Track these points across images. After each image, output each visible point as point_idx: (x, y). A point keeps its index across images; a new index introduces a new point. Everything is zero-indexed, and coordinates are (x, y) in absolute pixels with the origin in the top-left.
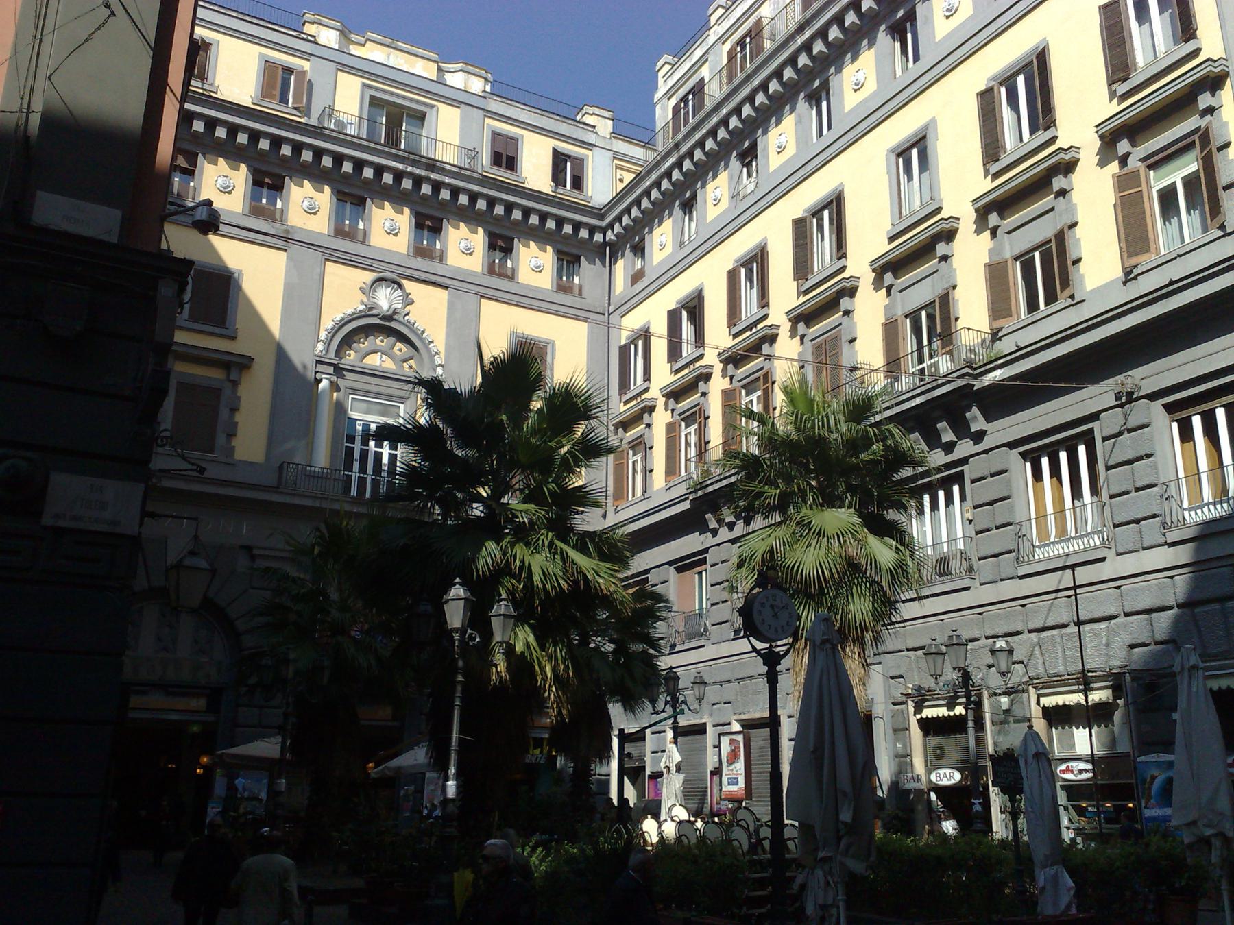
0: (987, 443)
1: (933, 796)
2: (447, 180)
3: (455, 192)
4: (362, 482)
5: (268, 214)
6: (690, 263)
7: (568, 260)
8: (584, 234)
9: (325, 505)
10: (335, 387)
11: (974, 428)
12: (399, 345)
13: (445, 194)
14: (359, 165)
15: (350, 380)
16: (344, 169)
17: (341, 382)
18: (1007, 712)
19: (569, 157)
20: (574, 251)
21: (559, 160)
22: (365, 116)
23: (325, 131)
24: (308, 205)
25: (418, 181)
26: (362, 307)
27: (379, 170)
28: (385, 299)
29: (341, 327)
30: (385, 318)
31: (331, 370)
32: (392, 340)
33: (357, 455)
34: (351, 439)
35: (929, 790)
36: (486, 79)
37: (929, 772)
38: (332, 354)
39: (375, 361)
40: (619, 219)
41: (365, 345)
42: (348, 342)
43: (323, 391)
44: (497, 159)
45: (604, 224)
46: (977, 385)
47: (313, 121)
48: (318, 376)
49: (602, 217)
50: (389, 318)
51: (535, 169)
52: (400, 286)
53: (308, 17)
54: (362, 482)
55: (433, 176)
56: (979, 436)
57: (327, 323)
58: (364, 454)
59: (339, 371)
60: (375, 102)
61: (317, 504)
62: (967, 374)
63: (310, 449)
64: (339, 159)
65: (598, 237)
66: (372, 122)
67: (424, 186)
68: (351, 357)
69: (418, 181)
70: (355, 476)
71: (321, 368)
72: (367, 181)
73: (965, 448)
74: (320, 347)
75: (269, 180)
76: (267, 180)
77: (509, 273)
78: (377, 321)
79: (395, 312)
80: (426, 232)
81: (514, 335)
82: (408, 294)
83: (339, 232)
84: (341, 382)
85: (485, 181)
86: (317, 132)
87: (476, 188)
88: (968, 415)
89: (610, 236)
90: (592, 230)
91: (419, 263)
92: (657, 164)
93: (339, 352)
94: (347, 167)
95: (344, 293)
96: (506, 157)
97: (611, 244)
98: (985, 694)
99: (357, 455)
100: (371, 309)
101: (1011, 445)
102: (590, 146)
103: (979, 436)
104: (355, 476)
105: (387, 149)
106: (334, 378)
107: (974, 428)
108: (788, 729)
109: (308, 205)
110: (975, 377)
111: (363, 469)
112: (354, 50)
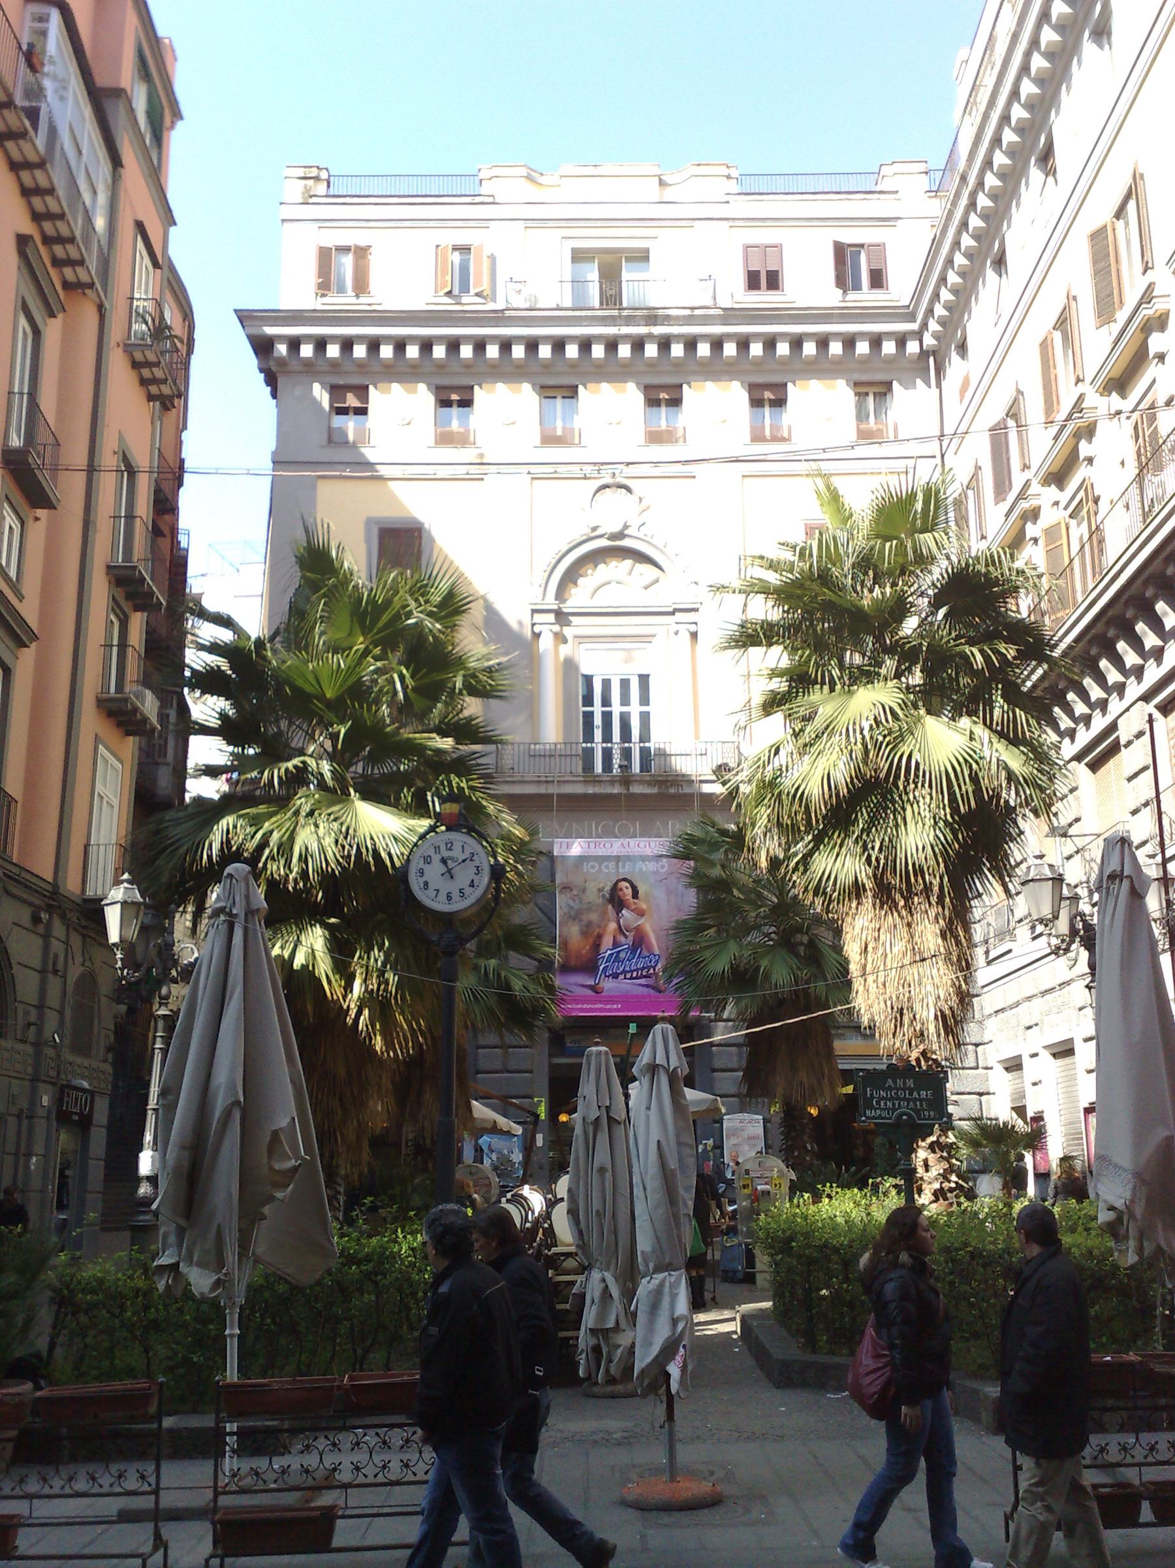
3: (691, 344)
4: (607, 755)
6: (1009, 347)
7: (874, 389)
8: (889, 347)
9: (553, 790)
10: (560, 638)
13: (677, 350)
14: (559, 345)
17: (568, 632)
19: (862, 246)
21: (844, 255)
23: (508, 313)
25: (638, 345)
27: (585, 345)
28: (612, 513)
31: (551, 618)
32: (628, 563)
33: (598, 720)
34: (588, 700)
39: (608, 599)
40: (930, 311)
42: (571, 577)
44: (753, 281)
45: (914, 326)
47: (500, 305)
48: (537, 629)
49: (911, 317)
50: (620, 535)
51: (810, 283)
52: (629, 490)
54: (607, 755)
58: (607, 717)
60: (578, 256)
61: (542, 790)
64: (532, 345)
65: (913, 347)
66: (578, 283)
68: (578, 598)
69: (638, 345)
70: (598, 746)
71: (538, 618)
75: (454, 396)
76: (663, 396)
77: (785, 435)
78: (604, 543)
79: (626, 527)
80: (767, 410)
81: (369, 522)
84: (568, 632)
85: (730, 315)
86: (498, 317)
87: (717, 330)
89: (929, 340)
90: (901, 341)
92: (950, 214)
93: (560, 594)
94: (863, 348)
96: (764, 278)
99: (598, 720)
100: (594, 529)
104: (598, 746)
106: (557, 628)
108: (68, 1013)
111: (607, 738)
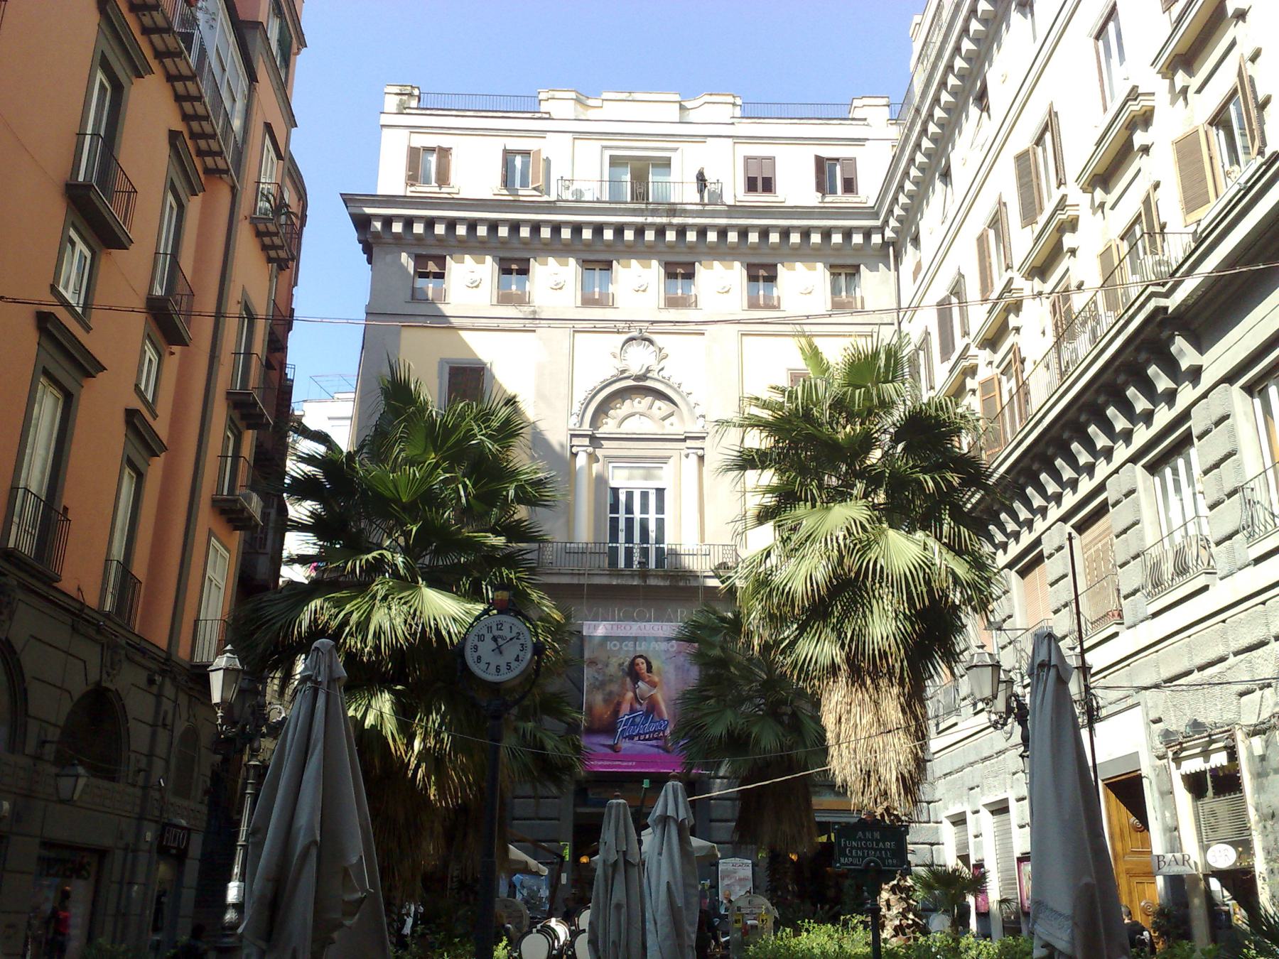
0: (1207, 380)
1: (1215, 884)
2: (690, 221)
3: (702, 232)
4: (629, 552)
5: (519, 300)
6: (952, 240)
7: (844, 272)
8: (858, 239)
9: (584, 581)
10: (593, 458)
11: (1184, 365)
12: (658, 403)
13: (691, 236)
14: (598, 229)
15: (609, 448)
16: (500, 234)
17: (599, 453)
18: (1263, 758)
19: (837, 160)
20: (850, 261)
21: (823, 166)
22: (606, 178)
23: (559, 204)
24: (554, 281)
25: (661, 231)
26: (615, 372)
27: (619, 230)
28: (638, 359)
29: (594, 396)
30: (637, 378)
31: (586, 441)
32: (649, 399)
33: (622, 525)
34: (615, 508)
35: (1206, 876)
36: (734, 104)
37: (1205, 848)
38: (586, 425)
39: (632, 427)
40: (891, 211)
41: (627, 406)
42: (603, 409)
43: (581, 468)
44: (751, 185)
45: (878, 223)
46: (1172, 303)
47: (553, 197)
48: (574, 450)
49: (876, 216)
50: (644, 377)
51: (796, 186)
52: (651, 342)
53: (542, 96)
54: (629, 552)
55: (676, 220)
56: (1195, 374)
57: (580, 395)
58: (630, 522)
59: (595, 441)
60: (615, 162)
61: (575, 581)
62: (1153, 295)
63: (570, 524)
64: (577, 229)
65: (876, 239)
66: (614, 182)
67: (688, 234)
68: (609, 426)
69: (661, 231)
70: (622, 546)
71: (576, 441)
72: (397, 236)
73: (1187, 394)
74: (574, 419)
75: (514, 266)
76: (680, 270)
77: (776, 303)
78: (630, 383)
79: (648, 370)
80: (761, 284)
81: (442, 362)
82: (660, 350)
83: (588, 301)
84: (599, 453)
85: (734, 211)
86: (551, 207)
87: (723, 221)
88: (1173, 349)
89: (889, 234)
90: (867, 233)
91: (674, 314)
92: (907, 138)
93: (595, 422)
94: (837, 238)
95: (600, 360)
96: (760, 182)
97: (894, 243)
98: (1240, 736)
99: (622, 525)
100: (623, 371)
101: (1230, 378)
102: (860, 141)
103: (1195, 374)
104: (622, 546)
105: (637, 206)
106: (590, 449)
107: (1184, 365)
108: (173, 761)
109: (554, 281)
110: (1167, 295)
111: (629, 538)
112: (591, 114)
